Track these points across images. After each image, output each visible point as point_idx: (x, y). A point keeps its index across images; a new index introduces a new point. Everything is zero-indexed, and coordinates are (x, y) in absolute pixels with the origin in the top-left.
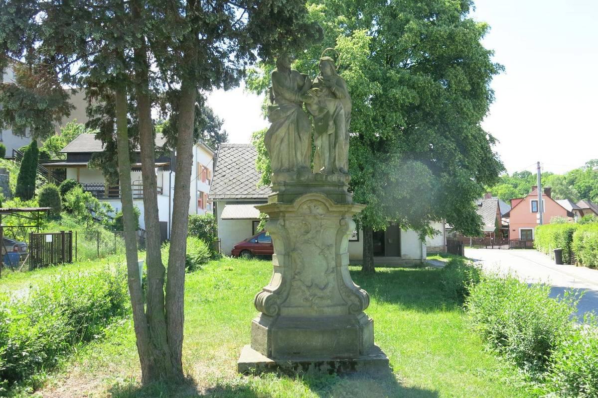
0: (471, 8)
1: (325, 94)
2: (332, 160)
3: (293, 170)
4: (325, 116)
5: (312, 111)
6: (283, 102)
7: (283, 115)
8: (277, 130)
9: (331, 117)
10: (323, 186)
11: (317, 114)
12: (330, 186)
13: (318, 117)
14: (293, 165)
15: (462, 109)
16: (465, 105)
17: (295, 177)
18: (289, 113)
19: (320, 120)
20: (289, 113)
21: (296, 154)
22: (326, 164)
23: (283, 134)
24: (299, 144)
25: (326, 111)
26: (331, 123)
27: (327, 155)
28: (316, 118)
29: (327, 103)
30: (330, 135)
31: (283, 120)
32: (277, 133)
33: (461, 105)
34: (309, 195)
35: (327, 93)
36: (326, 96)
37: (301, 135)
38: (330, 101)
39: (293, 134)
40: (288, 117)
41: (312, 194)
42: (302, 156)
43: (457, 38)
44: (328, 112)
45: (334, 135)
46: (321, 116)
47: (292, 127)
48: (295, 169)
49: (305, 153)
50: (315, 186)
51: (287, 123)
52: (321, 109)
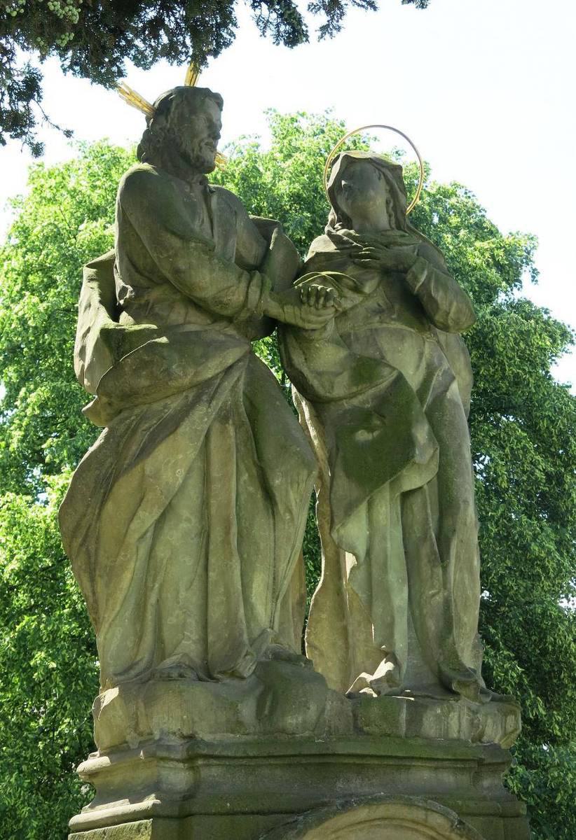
0: (525, 276)
1: (371, 304)
2: (432, 625)
3: (235, 675)
4: (383, 401)
5: (319, 374)
6: (178, 315)
7: (185, 376)
8: (145, 451)
9: (416, 400)
10: (403, 763)
11: (340, 388)
12: (435, 762)
13: (346, 405)
14: (235, 647)
15: (525, 548)
16: (535, 537)
17: (247, 711)
18: (211, 369)
19: (363, 418)
20: (211, 369)
21: (246, 587)
22: (401, 643)
23: (180, 473)
24: (261, 528)
25: (386, 379)
26: (422, 433)
27: (400, 598)
28: (333, 411)
29: (386, 344)
30: (406, 496)
31: (175, 404)
32: (149, 465)
33: (521, 535)
34: (363, 813)
35: (379, 300)
36: (379, 311)
37: (277, 482)
38: (401, 337)
39: (232, 483)
40: (204, 390)
41: (381, 811)
42: (275, 597)
43: (499, 346)
44: (400, 379)
45: (431, 496)
46: (366, 398)
47: (226, 443)
48: (247, 667)
49: (285, 588)
50: (360, 764)
51: (202, 416)
52: (364, 369)
